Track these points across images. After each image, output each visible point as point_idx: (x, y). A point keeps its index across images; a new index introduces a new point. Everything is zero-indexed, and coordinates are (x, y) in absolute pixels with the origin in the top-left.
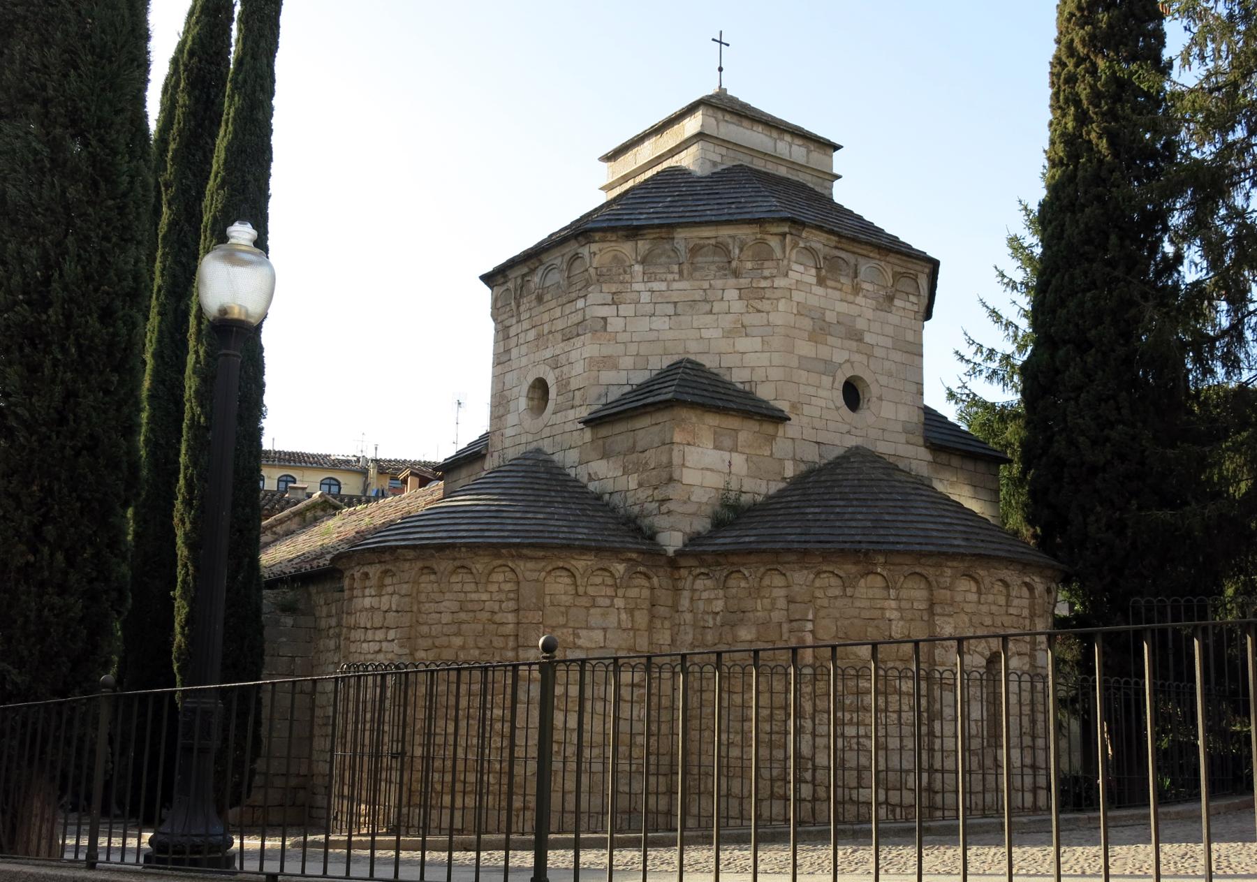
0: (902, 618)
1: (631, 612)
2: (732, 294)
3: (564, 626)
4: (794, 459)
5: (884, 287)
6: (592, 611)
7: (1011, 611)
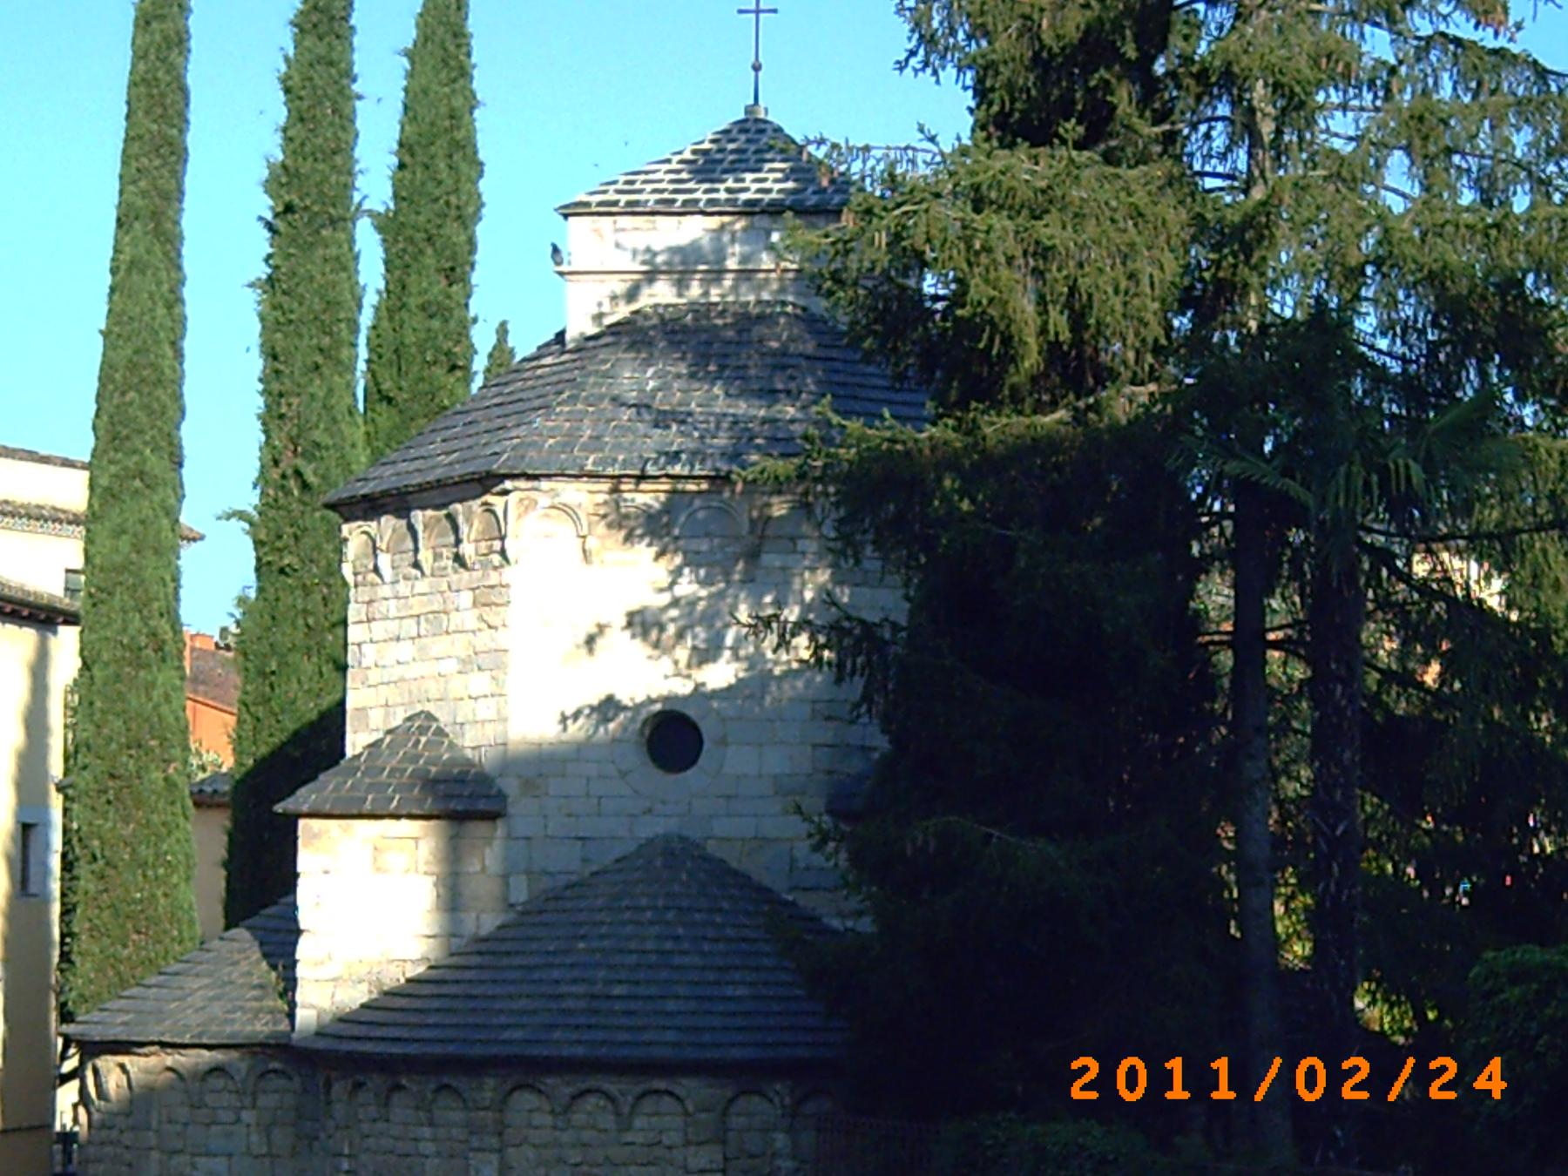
0: (438, 1154)
1: (267, 1130)
2: (466, 598)
3: (181, 1151)
4: (528, 872)
5: (737, 538)
6: (214, 1129)
7: (629, 1137)
